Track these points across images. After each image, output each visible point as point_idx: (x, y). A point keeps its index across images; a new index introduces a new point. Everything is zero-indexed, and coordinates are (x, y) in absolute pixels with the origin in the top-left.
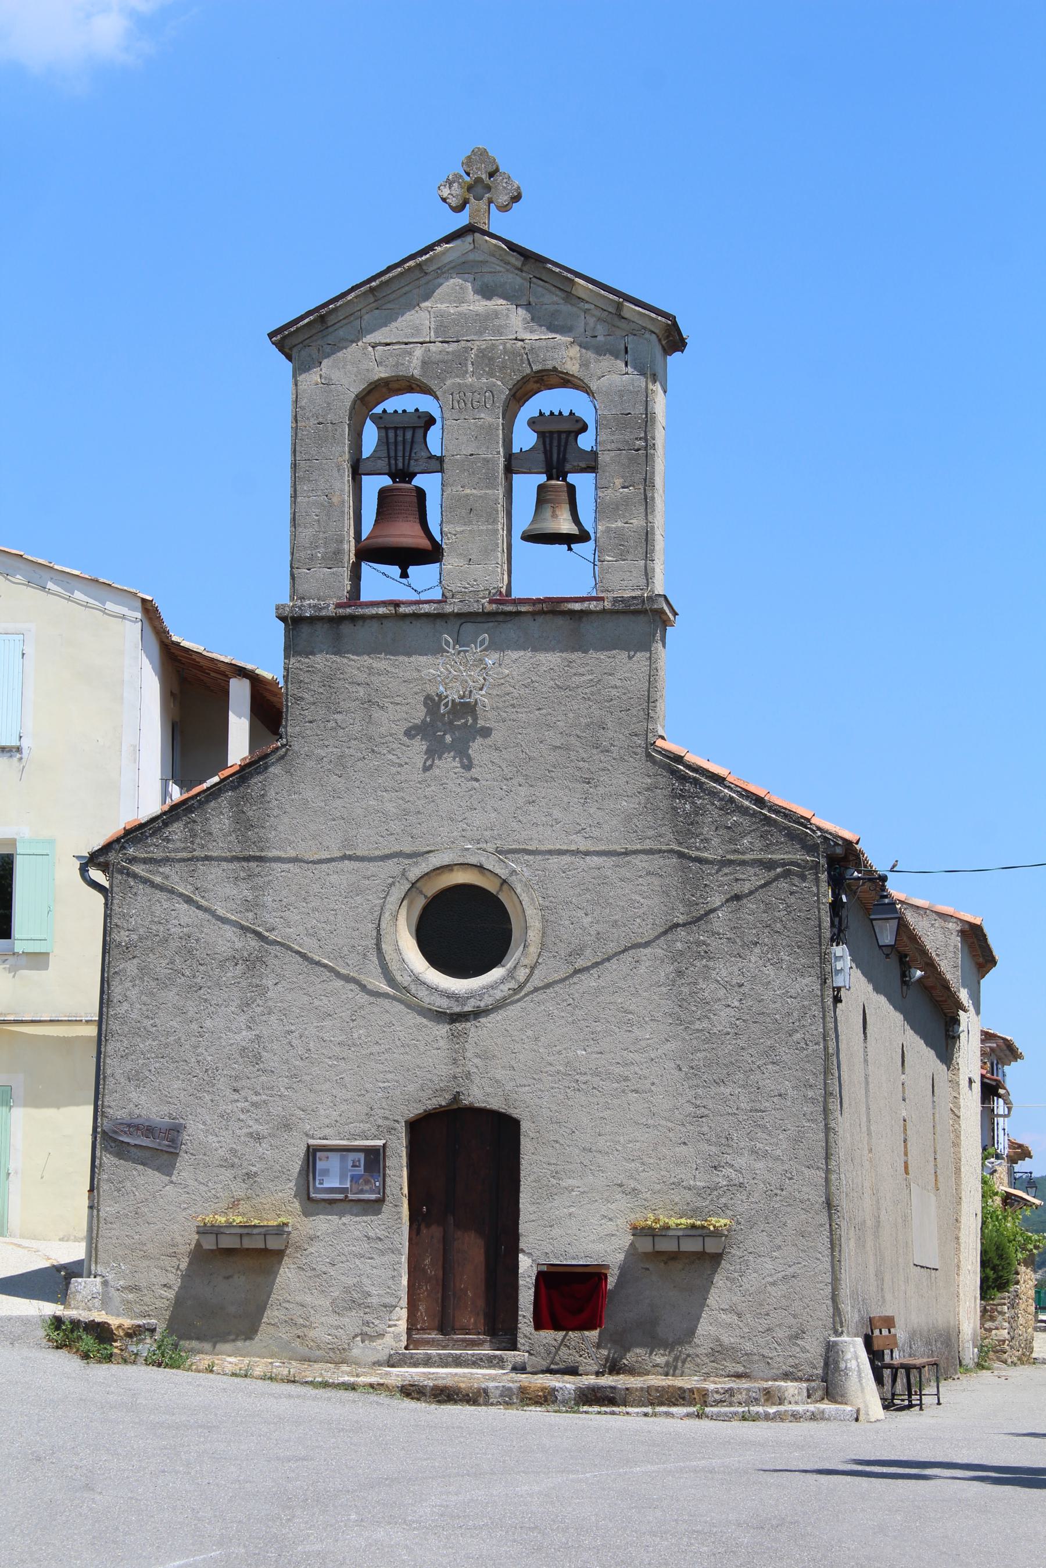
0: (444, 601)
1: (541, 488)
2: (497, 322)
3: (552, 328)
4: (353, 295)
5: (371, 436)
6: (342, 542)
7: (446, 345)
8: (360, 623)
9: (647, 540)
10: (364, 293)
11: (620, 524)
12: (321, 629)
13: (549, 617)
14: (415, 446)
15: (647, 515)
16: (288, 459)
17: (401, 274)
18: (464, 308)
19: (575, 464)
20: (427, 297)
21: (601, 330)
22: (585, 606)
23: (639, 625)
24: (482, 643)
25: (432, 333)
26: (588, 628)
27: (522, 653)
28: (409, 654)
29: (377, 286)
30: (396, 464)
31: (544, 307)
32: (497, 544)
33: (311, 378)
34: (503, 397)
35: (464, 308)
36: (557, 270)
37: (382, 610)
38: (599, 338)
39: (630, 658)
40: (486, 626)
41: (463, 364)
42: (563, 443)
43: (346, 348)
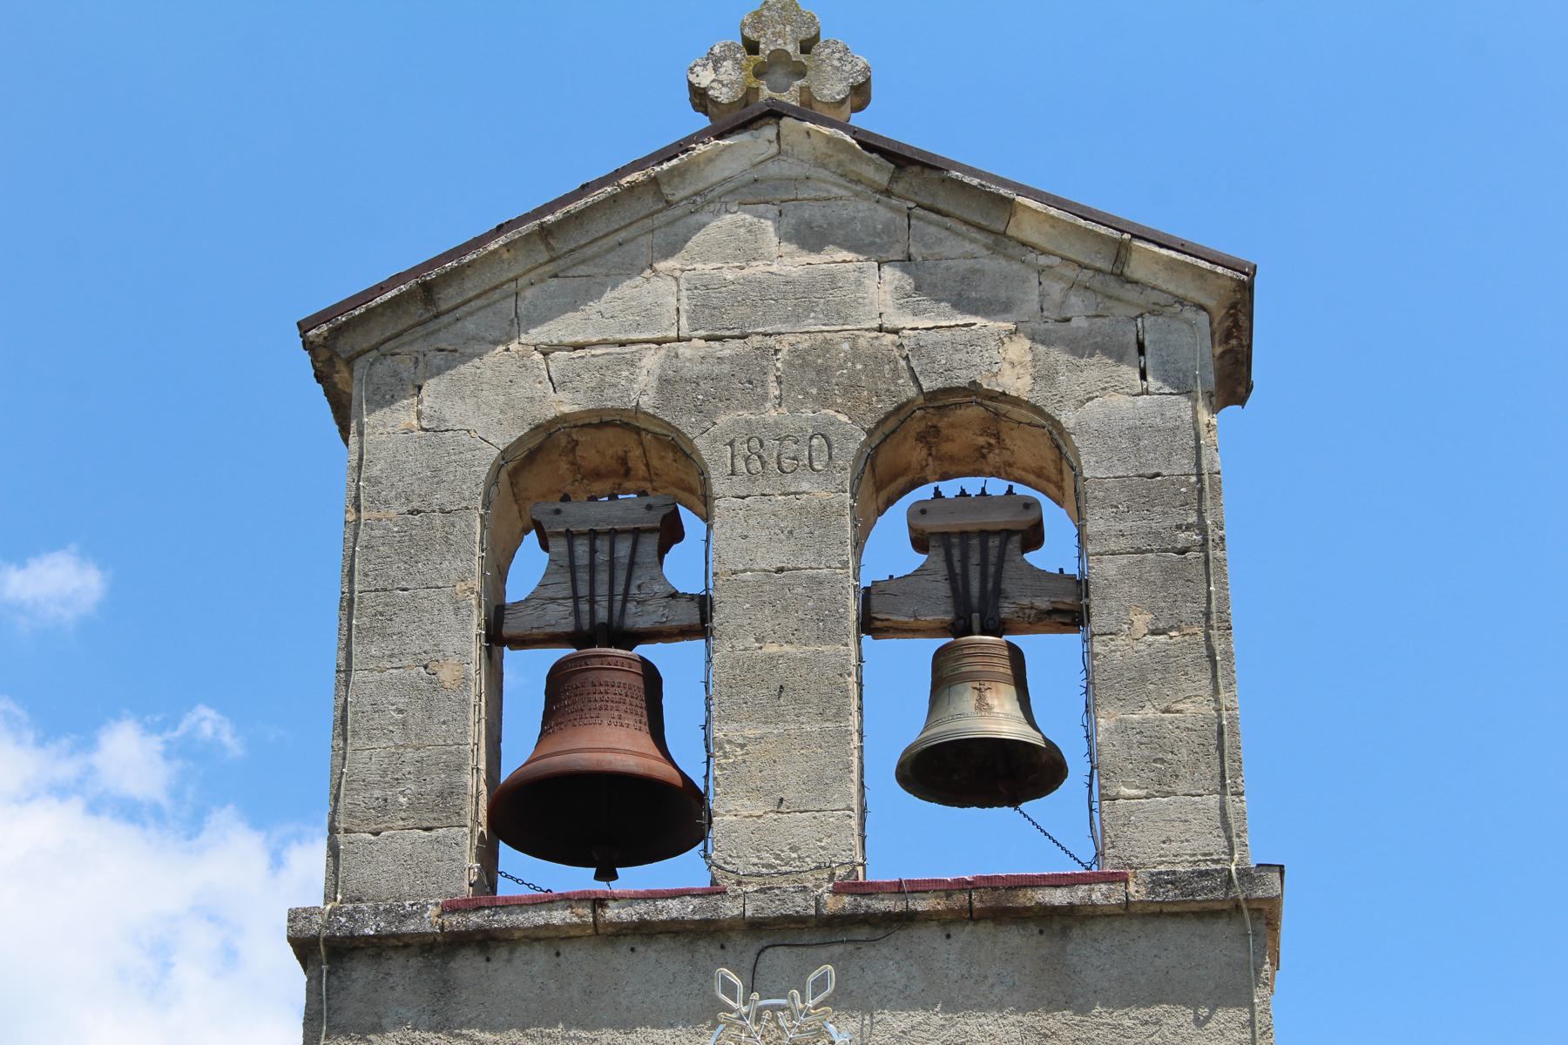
0: (715, 890)
1: (940, 656)
2: (835, 296)
3: (962, 304)
4: (502, 240)
5: (530, 566)
6: (459, 768)
7: (716, 345)
8: (502, 953)
9: (1220, 748)
10: (527, 238)
11: (1150, 713)
12: (402, 972)
13: (984, 929)
14: (637, 572)
15: (1216, 691)
16: (335, 587)
17: (614, 198)
18: (757, 269)
19: (1025, 602)
20: (671, 251)
21: (1078, 305)
22: (1079, 894)
23: (1216, 946)
24: (820, 984)
25: (684, 321)
26: (1089, 954)
27: (919, 1016)
28: (627, 1025)
29: (558, 223)
30: (592, 612)
31: (944, 264)
32: (848, 767)
33: (389, 426)
34: (854, 447)
35: (757, 269)
36: (975, 182)
37: (559, 916)
38: (1074, 323)
39: (1200, 1022)
40: (824, 953)
41: (754, 384)
42: (993, 557)
43: (480, 356)
